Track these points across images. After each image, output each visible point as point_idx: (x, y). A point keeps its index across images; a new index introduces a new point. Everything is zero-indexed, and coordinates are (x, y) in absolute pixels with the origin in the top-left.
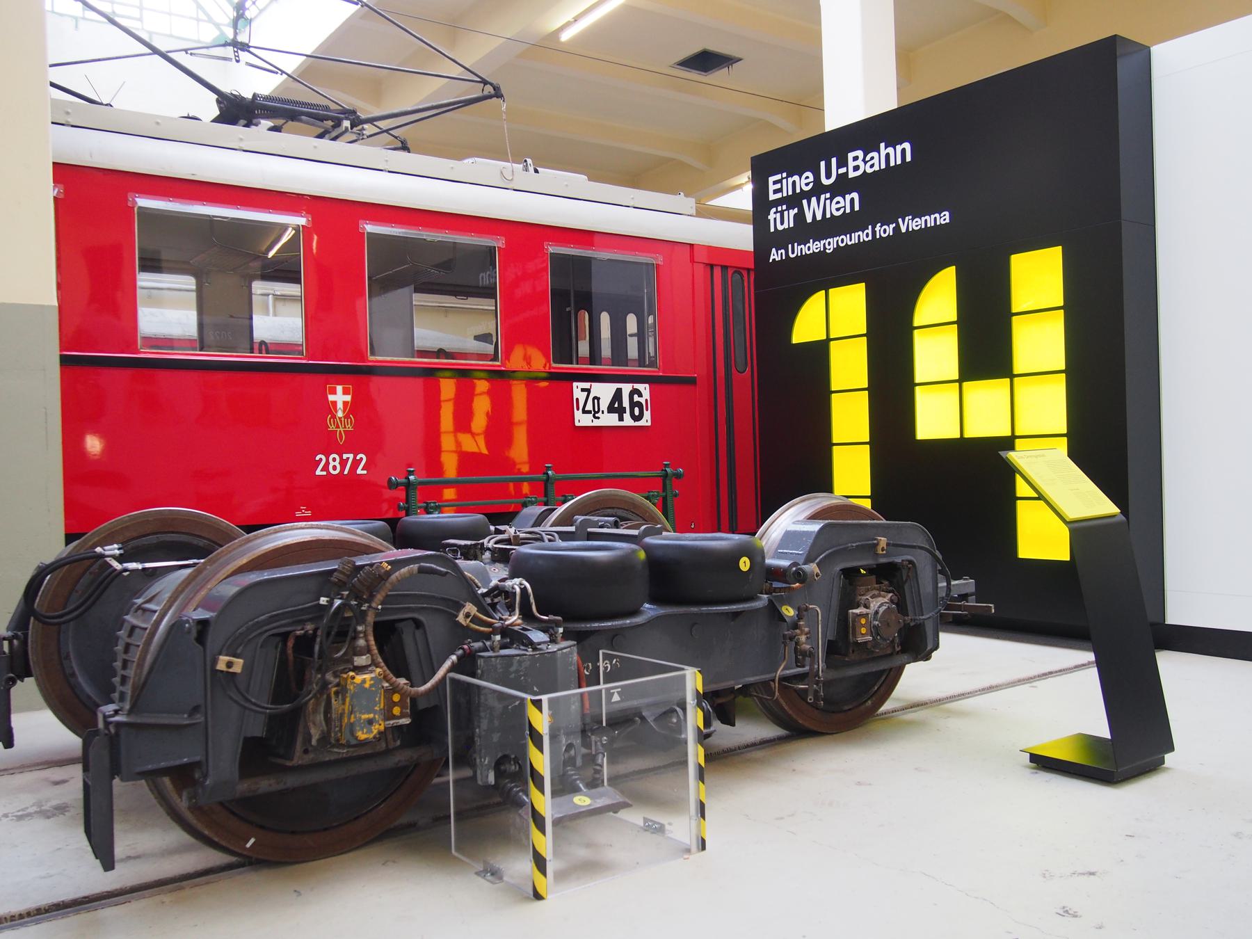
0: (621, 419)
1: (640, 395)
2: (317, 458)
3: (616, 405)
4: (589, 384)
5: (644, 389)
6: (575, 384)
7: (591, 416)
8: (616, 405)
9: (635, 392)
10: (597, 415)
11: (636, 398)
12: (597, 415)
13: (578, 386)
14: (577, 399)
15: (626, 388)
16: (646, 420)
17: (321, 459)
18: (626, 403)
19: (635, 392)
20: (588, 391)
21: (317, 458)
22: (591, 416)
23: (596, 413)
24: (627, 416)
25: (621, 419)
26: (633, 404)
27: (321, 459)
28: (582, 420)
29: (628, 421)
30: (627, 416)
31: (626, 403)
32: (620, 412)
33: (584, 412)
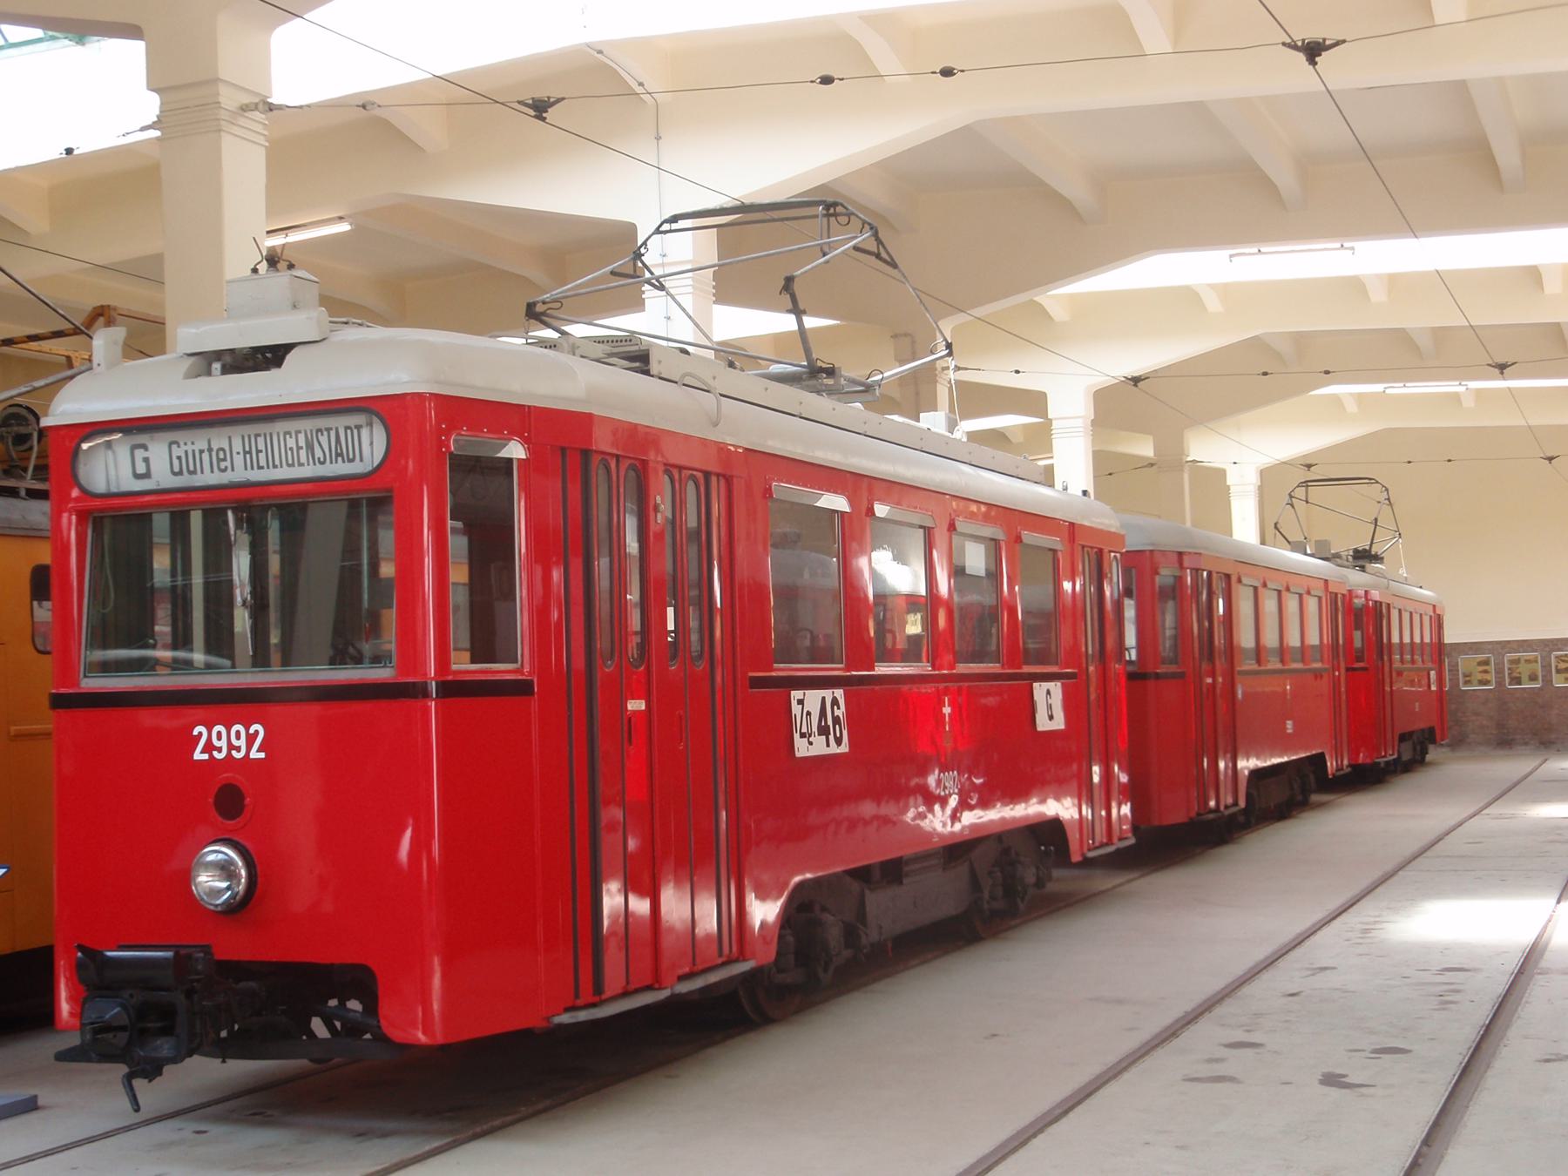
0: (828, 745)
1: (839, 708)
2: (195, 733)
3: (823, 724)
4: (802, 692)
5: (839, 693)
6: (793, 693)
7: (806, 739)
8: (823, 724)
9: (835, 702)
10: (811, 740)
11: (837, 713)
12: (811, 740)
13: (796, 694)
14: (795, 715)
15: (828, 694)
16: (844, 748)
17: (200, 734)
18: (830, 722)
19: (835, 702)
20: (801, 702)
21: (195, 733)
22: (806, 739)
23: (810, 736)
24: (831, 737)
25: (828, 745)
26: (836, 720)
27: (200, 734)
28: (802, 749)
29: (834, 749)
30: (831, 737)
31: (830, 722)
32: (824, 731)
33: (803, 735)
